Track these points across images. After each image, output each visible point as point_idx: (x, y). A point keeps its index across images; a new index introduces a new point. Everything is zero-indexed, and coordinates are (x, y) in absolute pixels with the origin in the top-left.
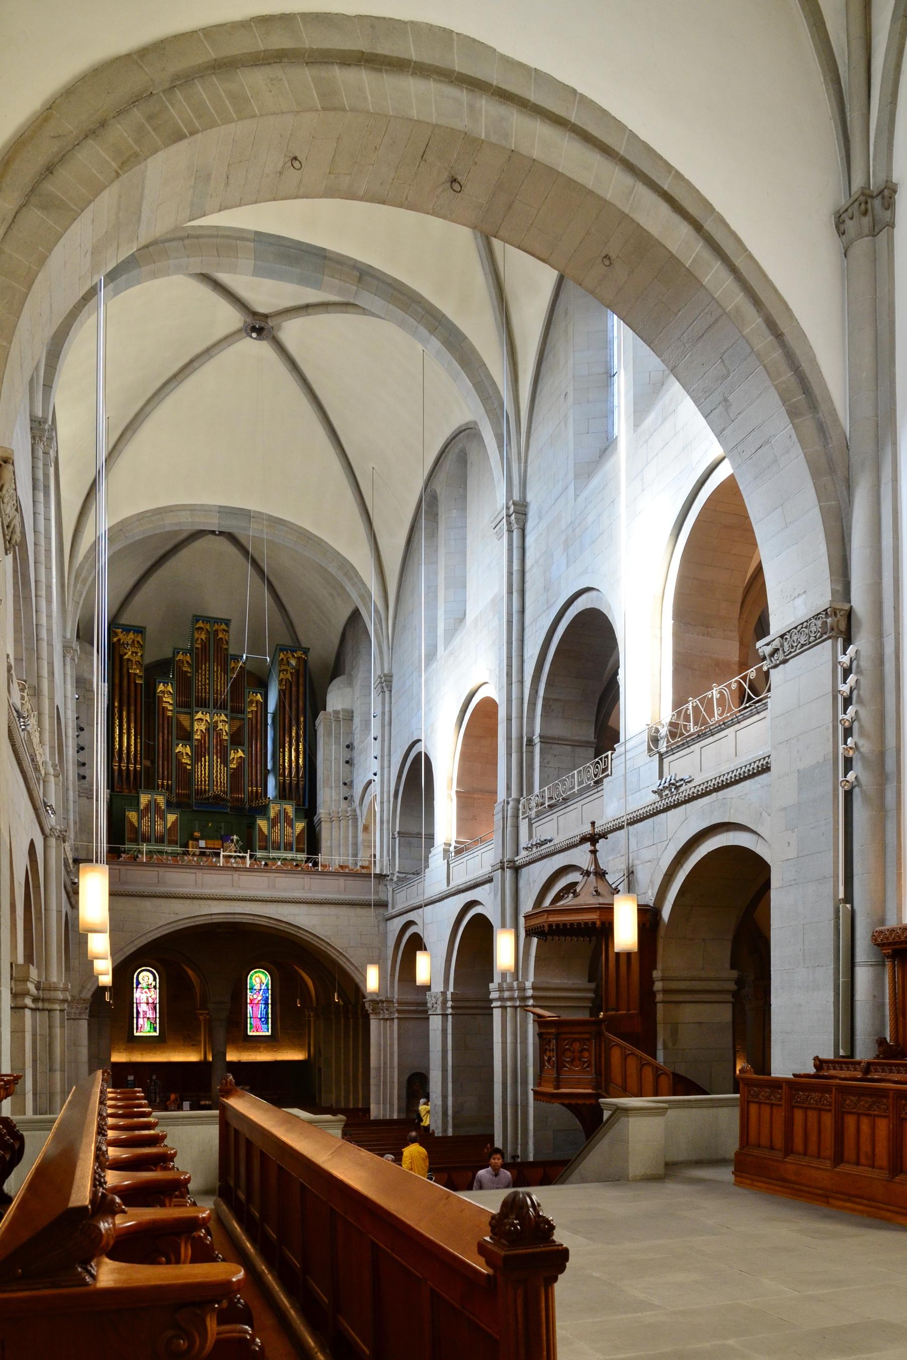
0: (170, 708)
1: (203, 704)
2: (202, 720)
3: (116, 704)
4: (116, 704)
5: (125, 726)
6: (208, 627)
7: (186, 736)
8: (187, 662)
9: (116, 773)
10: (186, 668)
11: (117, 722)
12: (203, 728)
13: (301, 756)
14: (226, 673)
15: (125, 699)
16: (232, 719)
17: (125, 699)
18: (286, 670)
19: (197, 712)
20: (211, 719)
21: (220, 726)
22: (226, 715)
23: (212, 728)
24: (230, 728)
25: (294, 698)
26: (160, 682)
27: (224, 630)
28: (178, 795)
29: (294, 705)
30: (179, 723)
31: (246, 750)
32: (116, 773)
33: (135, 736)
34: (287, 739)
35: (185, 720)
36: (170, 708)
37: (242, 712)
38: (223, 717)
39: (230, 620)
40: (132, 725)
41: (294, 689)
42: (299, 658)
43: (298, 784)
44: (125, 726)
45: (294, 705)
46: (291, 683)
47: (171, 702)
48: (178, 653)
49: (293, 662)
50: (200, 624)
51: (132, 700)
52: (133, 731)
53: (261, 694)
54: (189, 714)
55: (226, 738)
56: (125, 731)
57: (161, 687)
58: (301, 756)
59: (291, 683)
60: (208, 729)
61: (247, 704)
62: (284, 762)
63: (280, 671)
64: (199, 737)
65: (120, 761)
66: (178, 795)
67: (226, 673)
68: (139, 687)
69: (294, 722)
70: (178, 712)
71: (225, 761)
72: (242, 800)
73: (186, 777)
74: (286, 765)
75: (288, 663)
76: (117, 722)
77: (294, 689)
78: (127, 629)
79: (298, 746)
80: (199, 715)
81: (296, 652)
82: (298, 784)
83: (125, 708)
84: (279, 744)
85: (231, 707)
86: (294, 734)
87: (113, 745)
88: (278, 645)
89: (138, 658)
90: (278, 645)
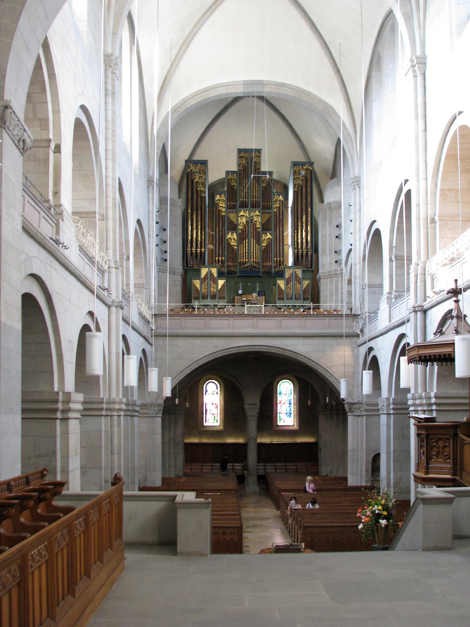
0: (224, 210)
1: (244, 206)
2: (244, 216)
3: (189, 211)
4: (189, 211)
5: (195, 225)
6: (247, 155)
7: (233, 227)
8: (234, 179)
9: (189, 255)
10: (234, 183)
11: (190, 222)
12: (244, 220)
13: (309, 235)
14: (259, 184)
15: (195, 208)
16: (263, 213)
17: (195, 208)
18: (299, 178)
19: (240, 211)
20: (249, 214)
21: (255, 219)
22: (259, 211)
23: (250, 221)
24: (261, 220)
25: (304, 196)
26: (217, 194)
27: (257, 156)
28: (228, 266)
29: (304, 201)
30: (228, 218)
31: (273, 233)
32: (189, 255)
33: (201, 230)
34: (300, 224)
35: (232, 216)
36: (224, 210)
37: (270, 208)
38: (257, 213)
39: (260, 150)
40: (199, 223)
41: (304, 190)
42: (306, 169)
43: (307, 253)
44: (195, 225)
45: (304, 201)
46: (302, 186)
47: (224, 206)
48: (229, 174)
49: (303, 173)
50: (242, 154)
51: (199, 207)
52: (199, 227)
53: (282, 195)
54: (236, 212)
55: (259, 226)
56: (194, 228)
57: (218, 197)
58: (309, 235)
59: (302, 186)
60: (247, 222)
61: (273, 203)
62: (298, 239)
63: (294, 179)
64: (241, 228)
65: (191, 247)
66: (228, 266)
67: (259, 184)
68: (203, 198)
69: (304, 213)
70: (228, 213)
71: (259, 242)
72: (270, 267)
73: (233, 253)
74: (299, 241)
75: (299, 173)
76: (190, 222)
77: (304, 190)
78: (196, 163)
79: (307, 227)
80: (242, 213)
81: (305, 165)
82: (307, 253)
83: (195, 213)
84: (295, 228)
85: (263, 205)
86: (304, 220)
87: (187, 237)
88: (293, 162)
89: (203, 181)
90: (293, 162)
